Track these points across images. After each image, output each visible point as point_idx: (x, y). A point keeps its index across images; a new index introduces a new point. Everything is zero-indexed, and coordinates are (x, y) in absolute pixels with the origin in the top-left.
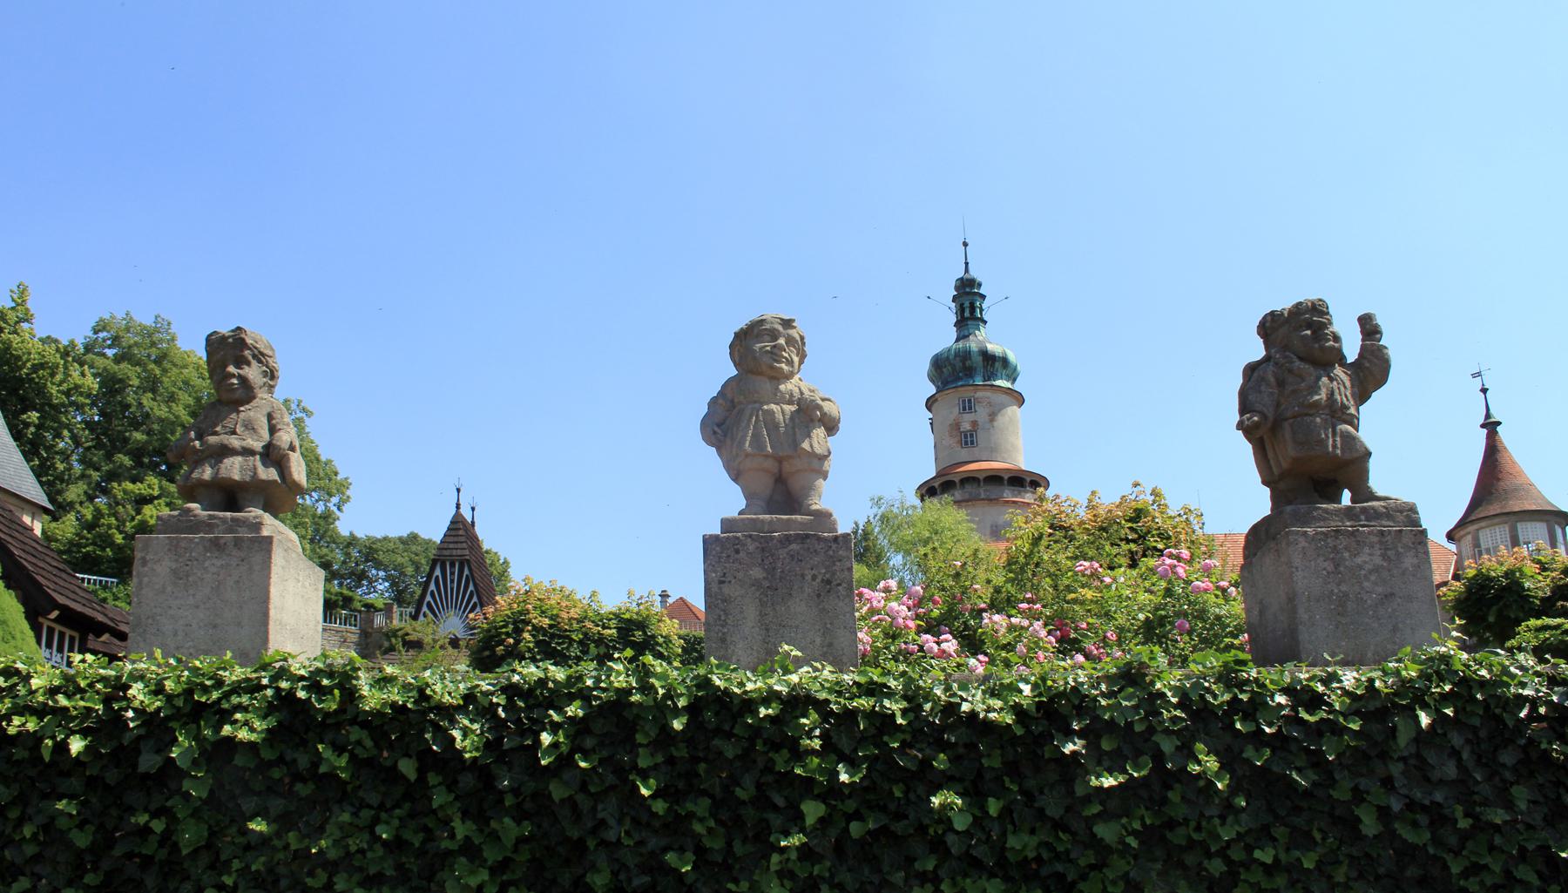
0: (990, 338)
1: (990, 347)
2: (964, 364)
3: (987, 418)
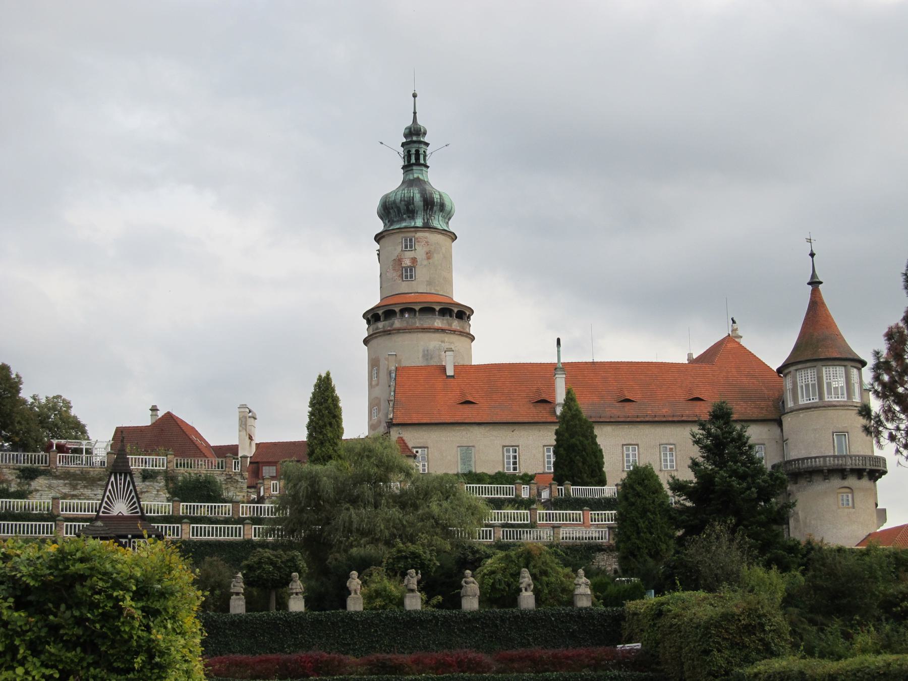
2: (408, 208)
3: (424, 256)
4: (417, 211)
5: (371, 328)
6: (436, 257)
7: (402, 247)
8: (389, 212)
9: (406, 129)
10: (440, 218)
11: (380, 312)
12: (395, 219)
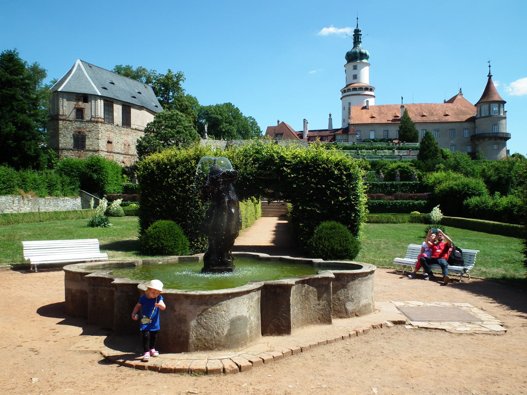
0: (363, 48)
1: (362, 50)
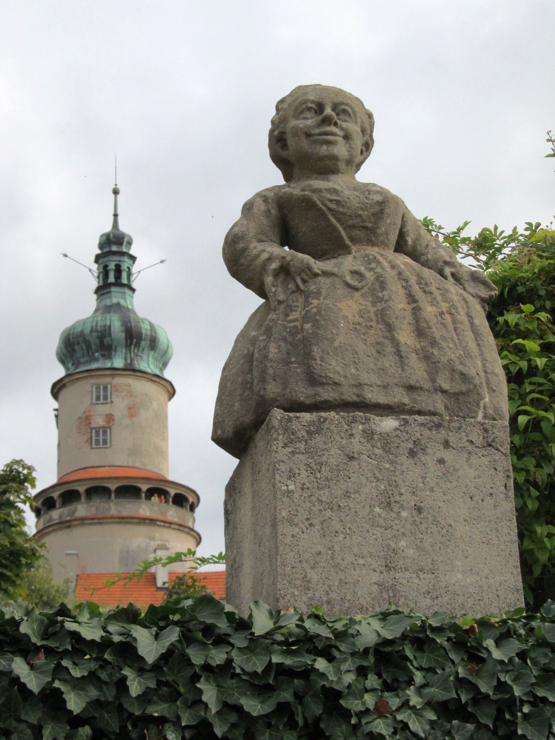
2: (102, 342)
4: (116, 347)
5: (42, 520)
6: (144, 415)
7: (92, 398)
8: (74, 350)
9: (102, 236)
10: (151, 360)
11: (55, 495)
12: (82, 360)
